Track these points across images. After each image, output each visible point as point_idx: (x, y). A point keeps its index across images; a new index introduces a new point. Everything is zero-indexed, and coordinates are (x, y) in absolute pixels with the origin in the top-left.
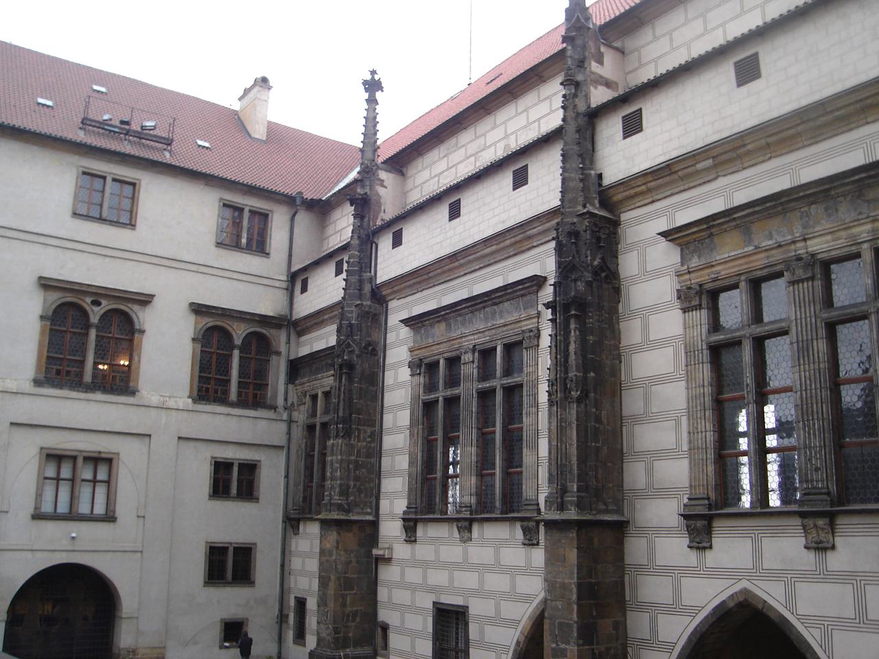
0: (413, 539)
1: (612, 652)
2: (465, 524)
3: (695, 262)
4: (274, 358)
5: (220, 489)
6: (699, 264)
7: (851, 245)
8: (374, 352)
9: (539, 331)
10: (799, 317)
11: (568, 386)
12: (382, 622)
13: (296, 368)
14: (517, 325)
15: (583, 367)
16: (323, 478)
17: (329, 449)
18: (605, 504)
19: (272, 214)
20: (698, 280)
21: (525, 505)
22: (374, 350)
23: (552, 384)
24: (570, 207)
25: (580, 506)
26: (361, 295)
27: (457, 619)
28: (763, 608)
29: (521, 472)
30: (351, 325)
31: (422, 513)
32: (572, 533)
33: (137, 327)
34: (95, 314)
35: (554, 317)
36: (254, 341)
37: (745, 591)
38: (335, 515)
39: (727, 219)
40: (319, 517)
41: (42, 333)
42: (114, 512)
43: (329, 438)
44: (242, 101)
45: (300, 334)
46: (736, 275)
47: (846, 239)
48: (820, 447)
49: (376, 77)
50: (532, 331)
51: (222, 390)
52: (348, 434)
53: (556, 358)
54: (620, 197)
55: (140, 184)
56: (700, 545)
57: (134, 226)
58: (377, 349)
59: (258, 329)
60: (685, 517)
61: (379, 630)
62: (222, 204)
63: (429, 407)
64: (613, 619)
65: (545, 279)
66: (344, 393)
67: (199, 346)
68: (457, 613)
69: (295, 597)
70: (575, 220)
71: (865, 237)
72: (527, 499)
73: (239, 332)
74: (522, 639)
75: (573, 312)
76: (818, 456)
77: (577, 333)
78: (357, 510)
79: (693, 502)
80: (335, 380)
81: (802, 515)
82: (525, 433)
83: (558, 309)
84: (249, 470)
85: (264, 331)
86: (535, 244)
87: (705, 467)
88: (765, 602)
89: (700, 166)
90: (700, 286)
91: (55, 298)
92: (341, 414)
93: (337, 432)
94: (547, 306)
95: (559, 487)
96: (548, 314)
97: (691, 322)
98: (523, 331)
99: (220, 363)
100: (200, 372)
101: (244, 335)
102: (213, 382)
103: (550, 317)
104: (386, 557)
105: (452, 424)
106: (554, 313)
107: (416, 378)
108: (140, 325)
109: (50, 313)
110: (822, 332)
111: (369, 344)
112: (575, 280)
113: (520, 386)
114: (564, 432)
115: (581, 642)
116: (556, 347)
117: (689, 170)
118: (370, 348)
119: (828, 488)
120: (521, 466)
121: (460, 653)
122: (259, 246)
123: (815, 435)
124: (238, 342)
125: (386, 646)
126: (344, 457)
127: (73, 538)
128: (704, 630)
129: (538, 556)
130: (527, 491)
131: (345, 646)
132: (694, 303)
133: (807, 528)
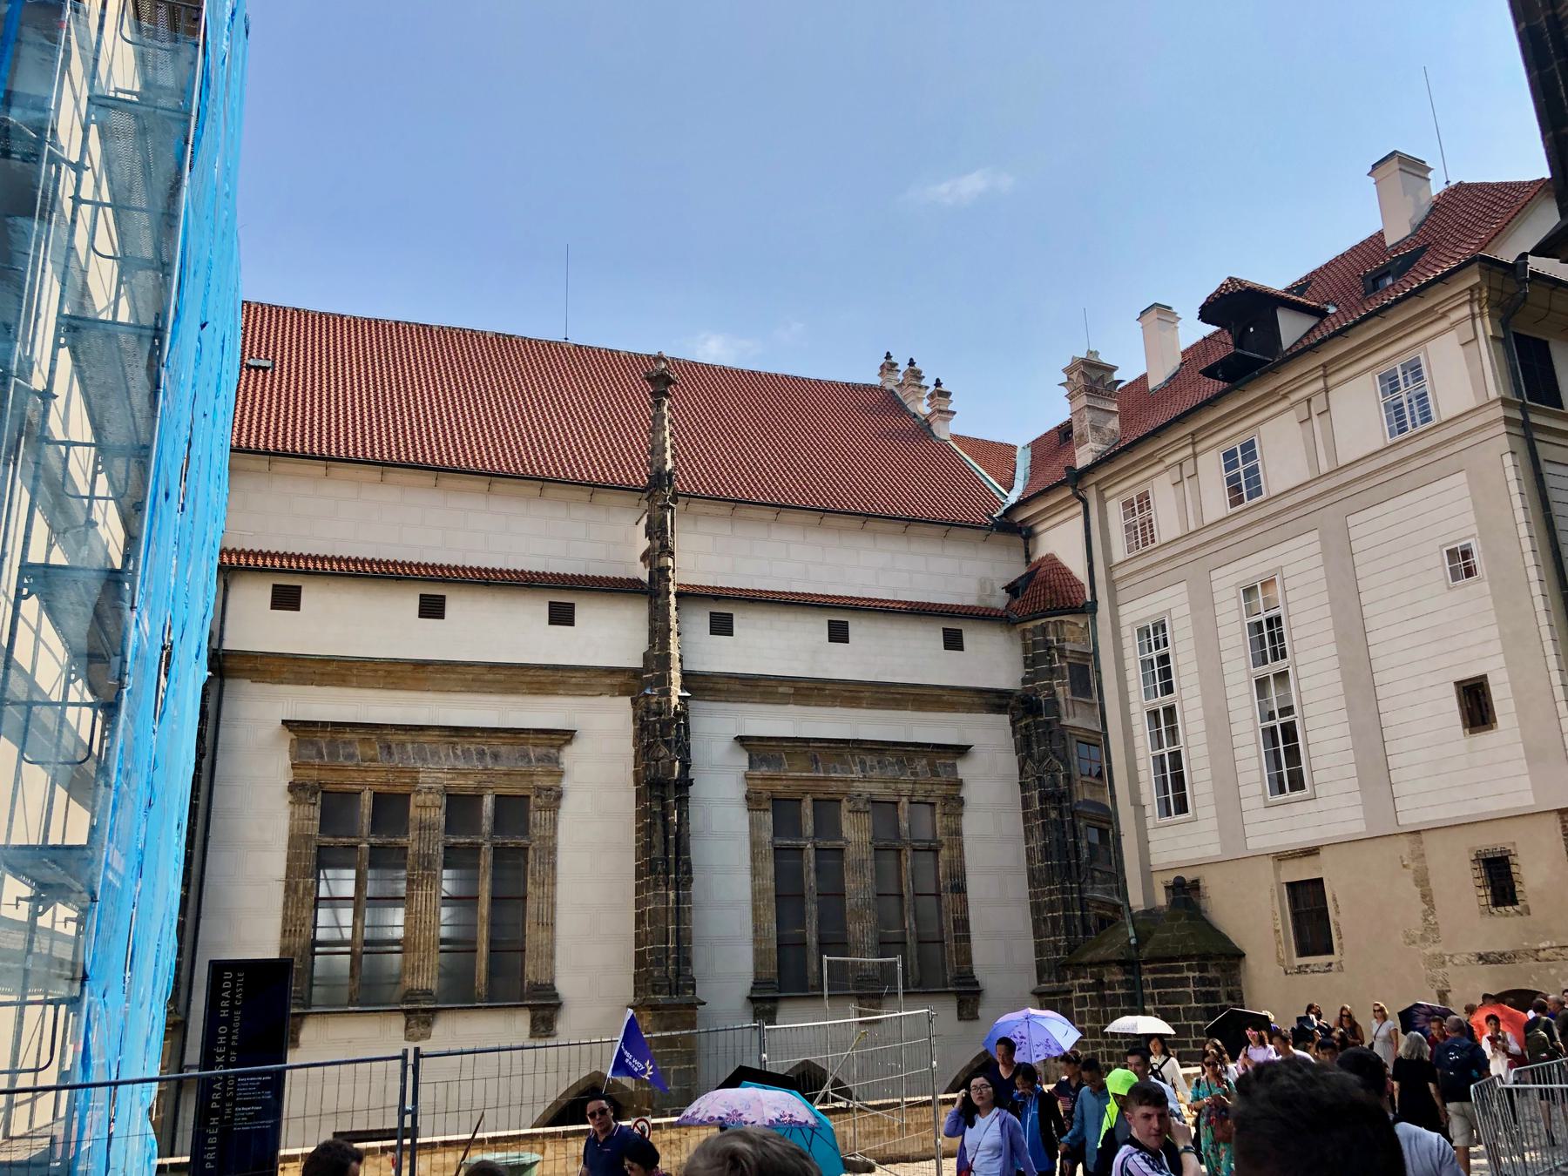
3: (764, 770)
50: (550, 790)
81: (860, 997)
89: (781, 690)
117: (770, 689)
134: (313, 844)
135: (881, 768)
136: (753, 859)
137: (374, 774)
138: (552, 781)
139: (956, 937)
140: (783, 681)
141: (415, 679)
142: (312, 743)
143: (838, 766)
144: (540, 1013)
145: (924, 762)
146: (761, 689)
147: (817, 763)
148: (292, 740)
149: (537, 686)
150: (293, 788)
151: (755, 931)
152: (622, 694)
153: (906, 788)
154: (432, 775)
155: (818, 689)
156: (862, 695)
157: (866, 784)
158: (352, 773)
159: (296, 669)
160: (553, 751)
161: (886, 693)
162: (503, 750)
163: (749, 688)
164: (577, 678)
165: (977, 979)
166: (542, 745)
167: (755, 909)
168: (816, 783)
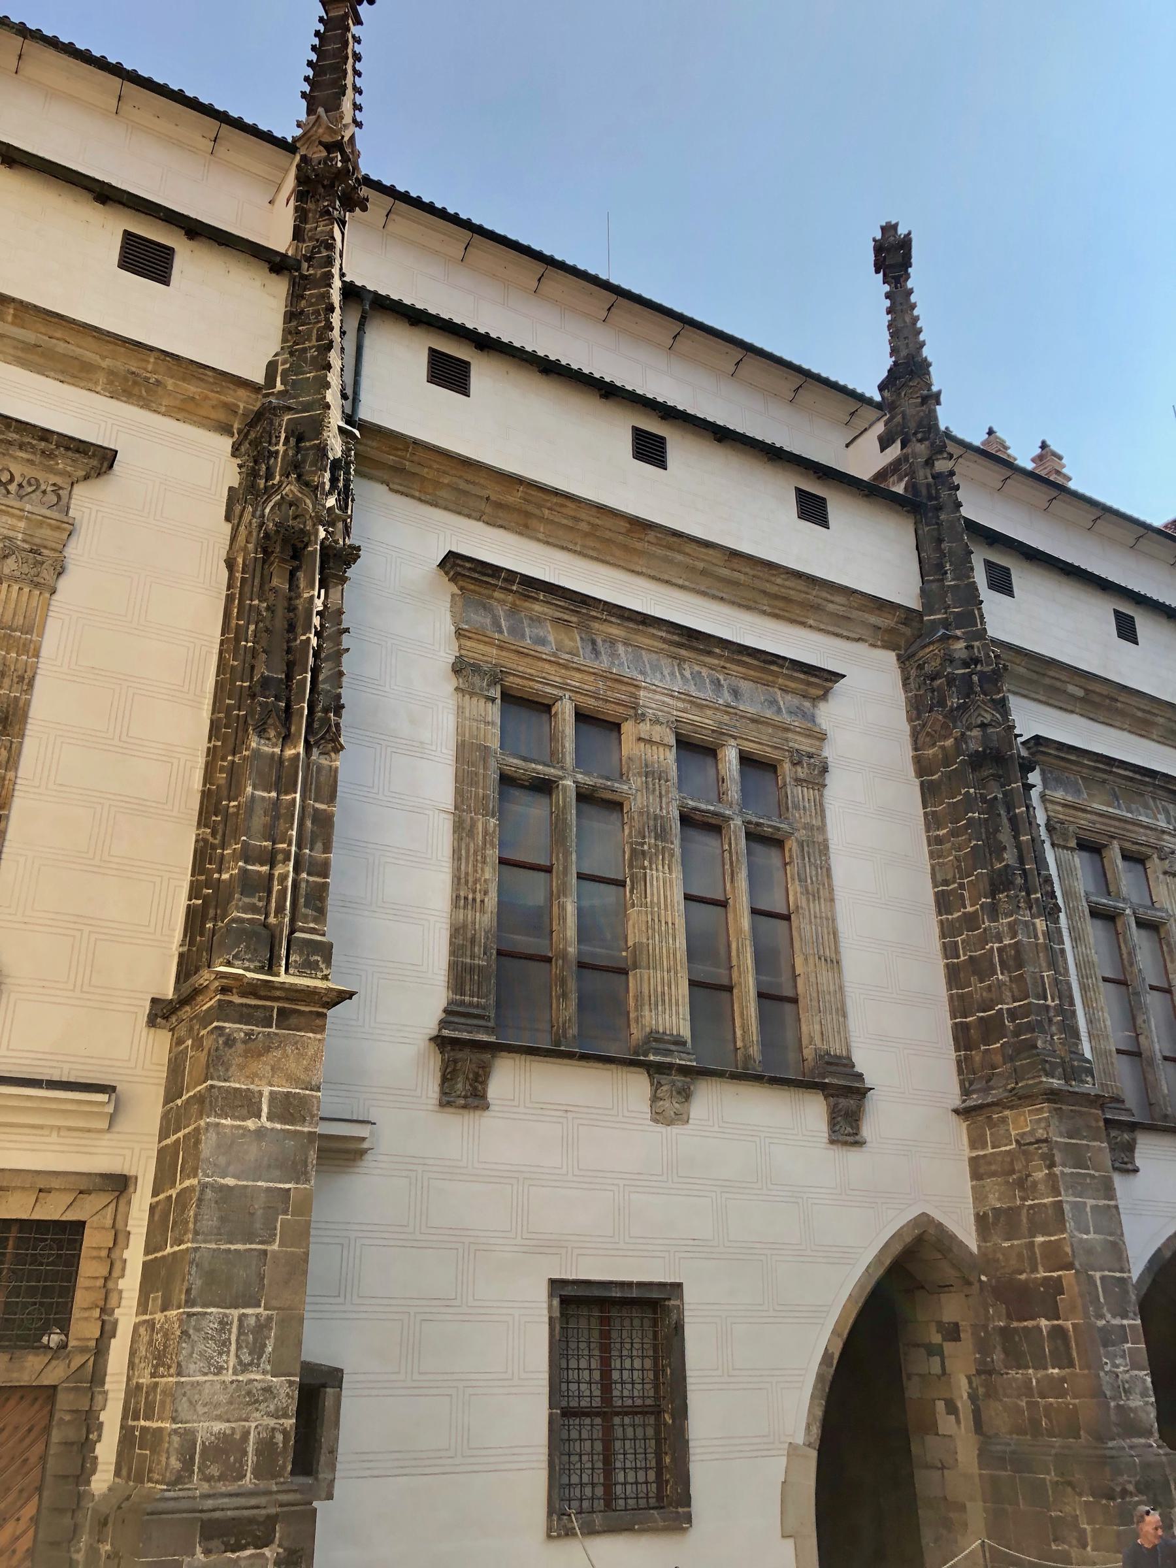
86: (811, 622)
134: (493, 764)
137: (578, 675)
141: (626, 548)
142: (485, 608)
144: (843, 1102)
148: (453, 595)
149: (781, 604)
150: (459, 668)
152: (887, 646)
154: (657, 697)
158: (547, 666)
160: (807, 704)
162: (744, 686)
164: (836, 605)
166: (793, 692)
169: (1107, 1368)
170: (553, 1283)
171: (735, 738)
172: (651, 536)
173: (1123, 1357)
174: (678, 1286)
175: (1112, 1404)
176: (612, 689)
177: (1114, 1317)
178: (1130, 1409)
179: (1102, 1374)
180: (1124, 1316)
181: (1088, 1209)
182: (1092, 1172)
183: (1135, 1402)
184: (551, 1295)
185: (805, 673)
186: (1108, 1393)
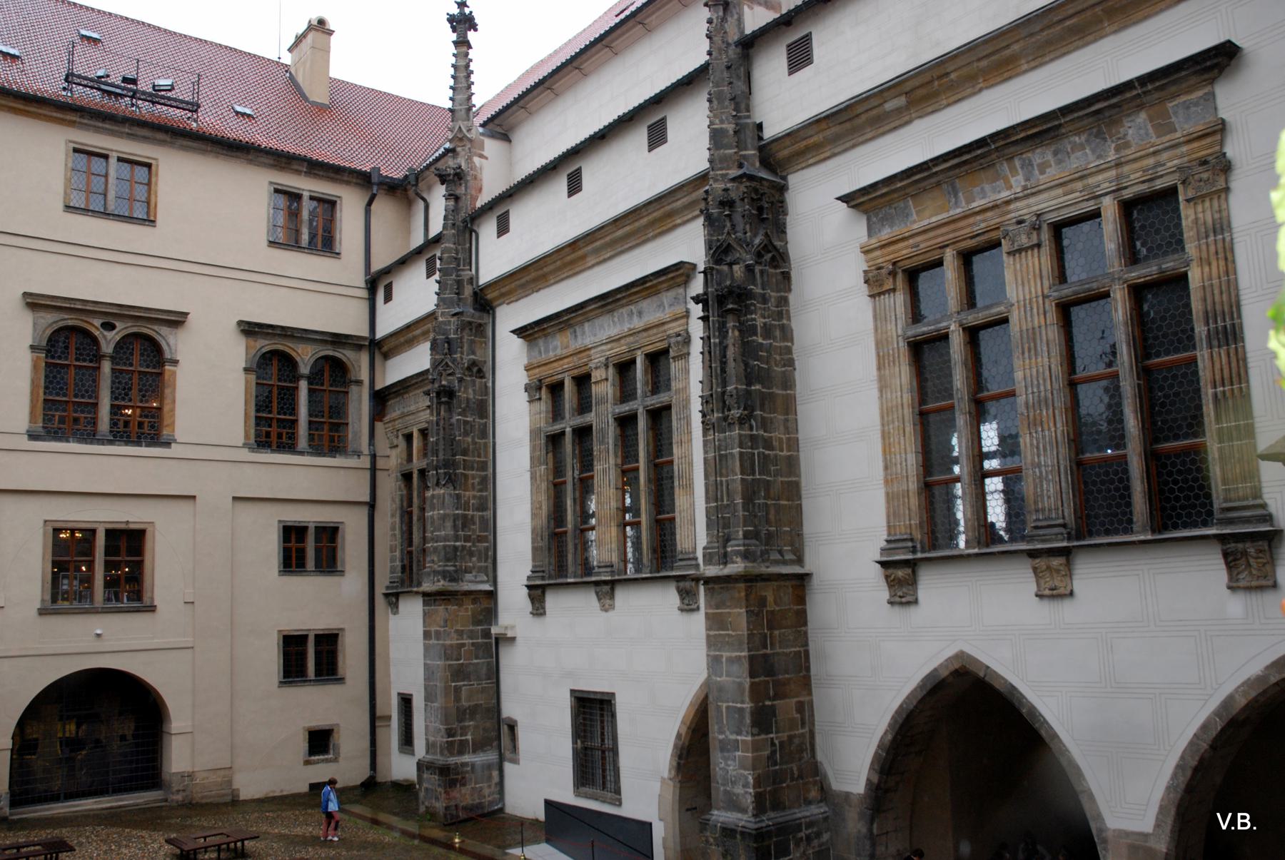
0: (542, 611)
1: (797, 741)
2: (607, 588)
3: (886, 233)
4: (354, 389)
5: (292, 561)
6: (891, 235)
7: (1087, 200)
8: (481, 374)
9: (688, 333)
10: (1022, 298)
11: (727, 403)
12: (509, 718)
13: (382, 399)
14: (662, 329)
15: (746, 377)
16: (424, 540)
17: (428, 503)
18: (780, 552)
19: (341, 201)
20: (892, 256)
21: (681, 560)
22: (480, 371)
23: (707, 402)
24: (721, 169)
25: (746, 556)
26: (460, 300)
27: (602, 709)
28: (985, 676)
29: (674, 519)
30: (449, 341)
31: (550, 577)
32: (739, 592)
33: (168, 355)
34: (108, 342)
35: (706, 314)
36: (327, 368)
37: (961, 655)
38: (441, 584)
39: (926, 174)
40: (421, 589)
41: (35, 367)
42: (152, 599)
43: (427, 488)
44: (295, 52)
45: (386, 356)
46: (940, 248)
47: (1081, 191)
48: (1053, 466)
49: (467, 11)
50: (679, 335)
51: (287, 433)
52: (452, 480)
53: (711, 367)
54: (785, 153)
55: (157, 166)
56: (904, 600)
57: (154, 221)
58: (484, 369)
59: (331, 353)
60: (883, 564)
61: (505, 729)
62: (272, 189)
63: (555, 440)
64: (795, 700)
65: (694, 266)
66: (444, 429)
67: (253, 377)
68: (602, 702)
69: (399, 694)
70: (729, 185)
71: (1106, 187)
72: (682, 552)
73: (306, 356)
74: (683, 732)
75: (730, 306)
76: (1050, 477)
77: (737, 333)
78: (468, 576)
79: (893, 546)
80: (432, 414)
82: (676, 468)
83: (710, 303)
84: (329, 534)
85: (337, 354)
86: (679, 221)
87: (906, 500)
88: (988, 667)
89: (889, 106)
90: (894, 264)
91: (50, 320)
92: (441, 457)
93: (438, 480)
94: (697, 299)
95: (720, 534)
96: (697, 310)
97: (883, 312)
98: (669, 337)
99: (282, 399)
100: (258, 411)
101: (312, 360)
102: (274, 424)
103: (701, 314)
104: (509, 635)
105: (586, 461)
106: (705, 309)
107: (537, 405)
108: (171, 353)
109: (44, 343)
110: (1052, 316)
111: (474, 363)
112: (730, 265)
113: (668, 408)
114: (724, 463)
115: (755, 731)
116: (710, 353)
118: (475, 369)
119: (1064, 518)
120: (673, 511)
121: (607, 753)
122: (325, 243)
123: (1045, 450)
124: (305, 369)
125: (515, 748)
126: (447, 511)
127: (98, 635)
128: (911, 707)
129: (697, 623)
130: (682, 541)
131: (461, 753)
132: (886, 287)
133: (1039, 571)
135: (1059, 162)
136: (879, 369)
138: (679, 326)
139: (1220, 431)
140: (881, 91)
143: (987, 187)
144: (682, 584)
145: (1142, 116)
146: (864, 117)
147: (956, 196)
151: (886, 468)
153: (1104, 181)
155: (940, 77)
156: (1007, 52)
157: (1032, 200)
159: (518, 283)
161: (1049, 27)
163: (848, 125)
165: (1273, 508)
167: (885, 435)
168: (952, 227)
169: (722, 765)
170: (572, 691)
171: (639, 348)
172: (580, 243)
173: (734, 760)
174: (613, 694)
175: (722, 788)
176: (580, 359)
177: (732, 733)
178: (734, 794)
179: (717, 769)
180: (739, 733)
181: (724, 659)
182: (730, 632)
183: (739, 790)
184: (571, 696)
185: (664, 275)
186: (720, 782)
